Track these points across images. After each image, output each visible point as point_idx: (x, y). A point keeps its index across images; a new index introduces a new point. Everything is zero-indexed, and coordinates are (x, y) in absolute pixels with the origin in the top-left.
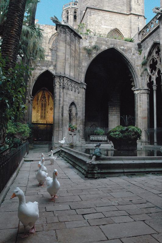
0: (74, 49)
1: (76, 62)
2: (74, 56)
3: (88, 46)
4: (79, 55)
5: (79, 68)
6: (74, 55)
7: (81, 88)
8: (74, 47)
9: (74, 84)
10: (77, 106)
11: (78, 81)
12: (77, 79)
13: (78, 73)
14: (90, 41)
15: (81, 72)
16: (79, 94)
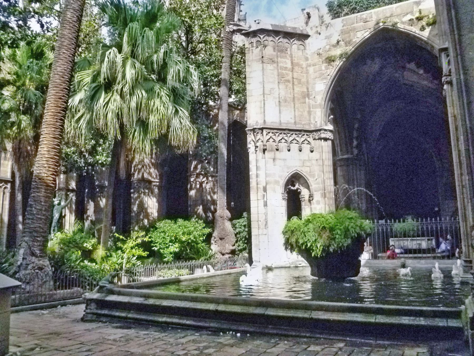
0: (289, 66)
1: (297, 89)
2: (291, 80)
3: (325, 47)
4: (307, 72)
5: (309, 99)
6: (290, 77)
7: (315, 139)
8: (289, 62)
9: (294, 136)
11: (307, 128)
12: (305, 124)
13: (307, 109)
14: (328, 34)
15: (315, 107)
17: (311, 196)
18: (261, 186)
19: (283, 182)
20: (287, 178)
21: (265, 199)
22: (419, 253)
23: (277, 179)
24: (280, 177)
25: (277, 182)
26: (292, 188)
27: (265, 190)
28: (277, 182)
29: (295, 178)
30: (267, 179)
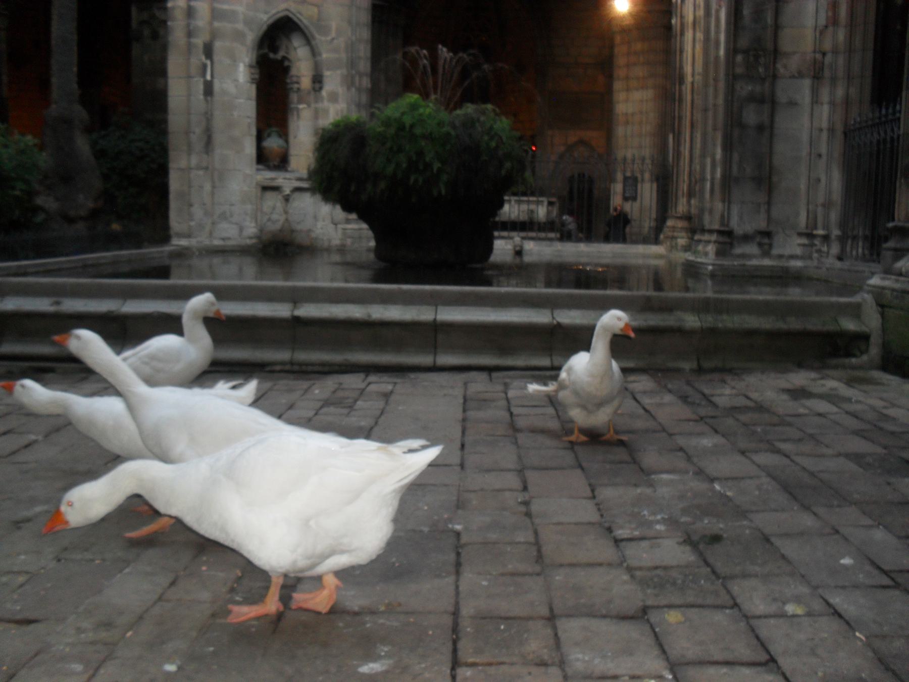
10: (320, 39)
17: (318, 80)
18: (199, 41)
19: (251, 37)
20: (265, 28)
21: (208, 77)
22: (531, 230)
23: (240, 26)
24: (248, 22)
25: (239, 36)
26: (272, 55)
27: (208, 51)
28: (239, 36)
29: (281, 30)
30: (216, 24)
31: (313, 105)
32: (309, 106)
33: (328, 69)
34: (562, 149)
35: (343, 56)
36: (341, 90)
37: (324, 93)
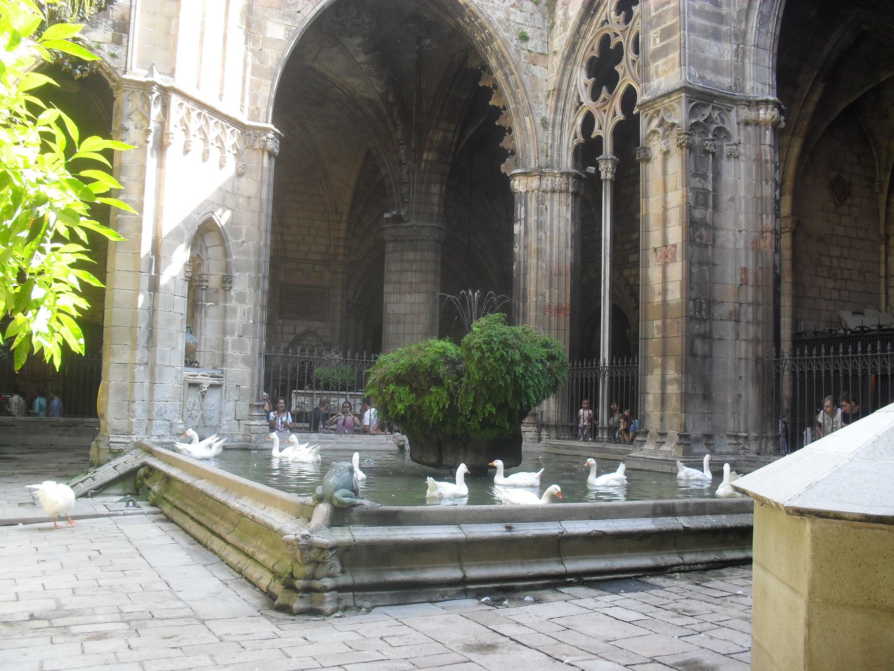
16: (243, 179)
17: (227, 281)
21: (153, 274)
31: (221, 304)
32: (217, 304)
33: (237, 271)
34: (291, 338)
35: (252, 259)
36: (248, 291)
37: (232, 293)
